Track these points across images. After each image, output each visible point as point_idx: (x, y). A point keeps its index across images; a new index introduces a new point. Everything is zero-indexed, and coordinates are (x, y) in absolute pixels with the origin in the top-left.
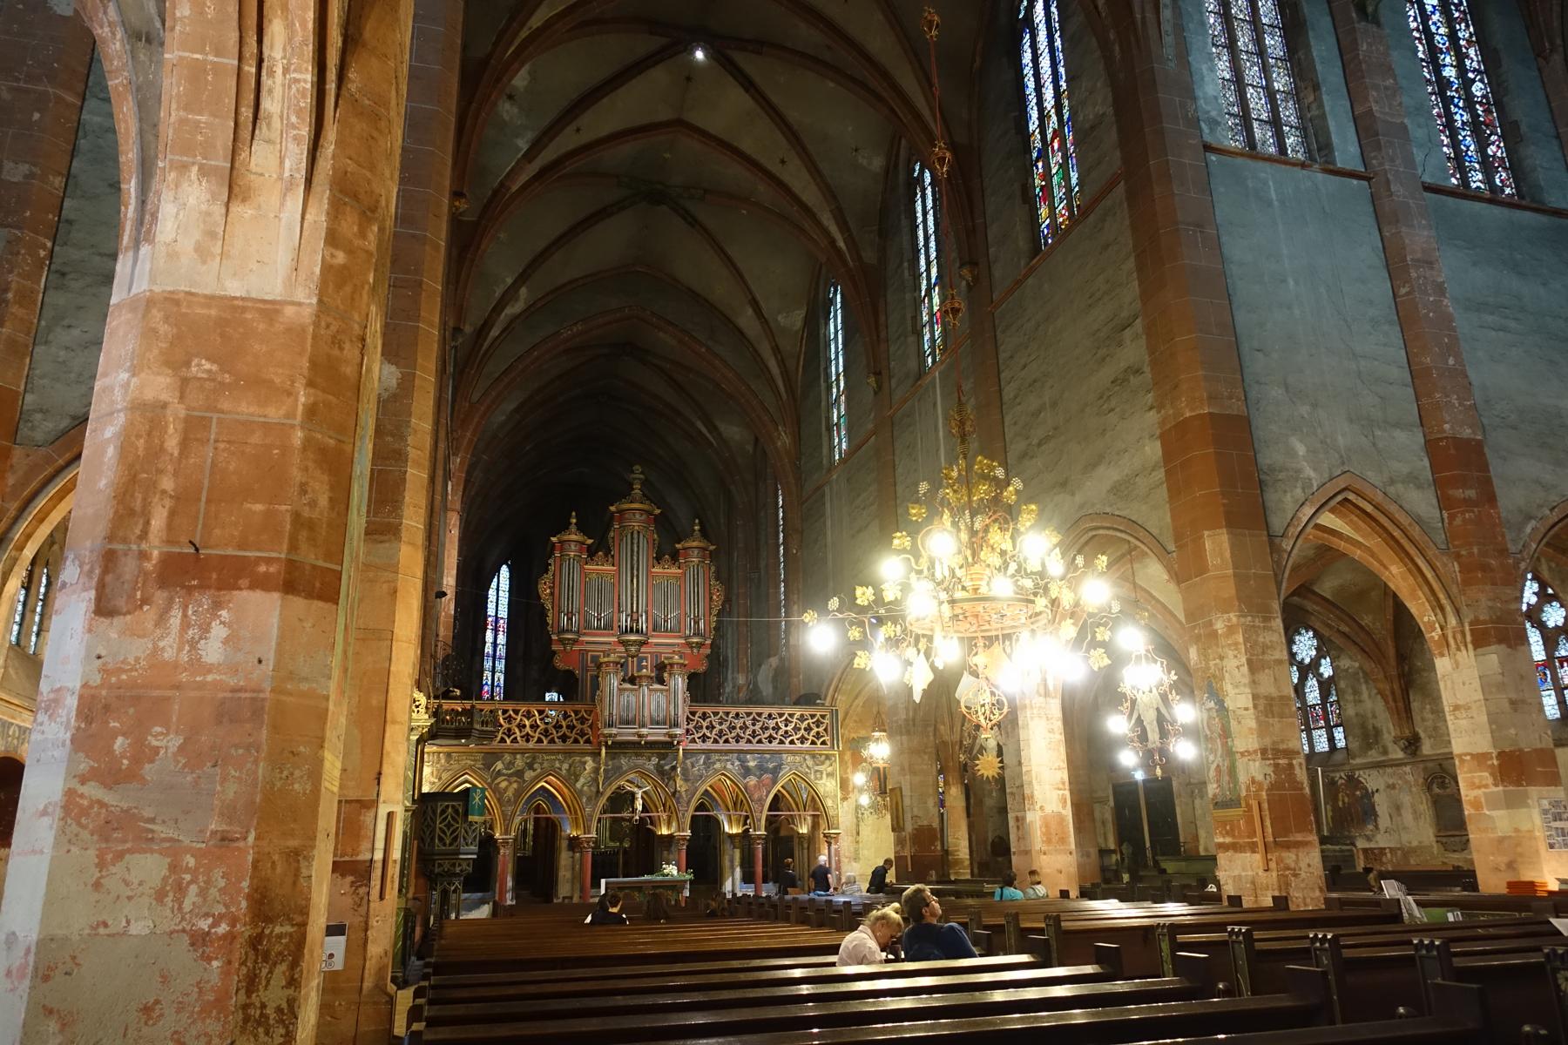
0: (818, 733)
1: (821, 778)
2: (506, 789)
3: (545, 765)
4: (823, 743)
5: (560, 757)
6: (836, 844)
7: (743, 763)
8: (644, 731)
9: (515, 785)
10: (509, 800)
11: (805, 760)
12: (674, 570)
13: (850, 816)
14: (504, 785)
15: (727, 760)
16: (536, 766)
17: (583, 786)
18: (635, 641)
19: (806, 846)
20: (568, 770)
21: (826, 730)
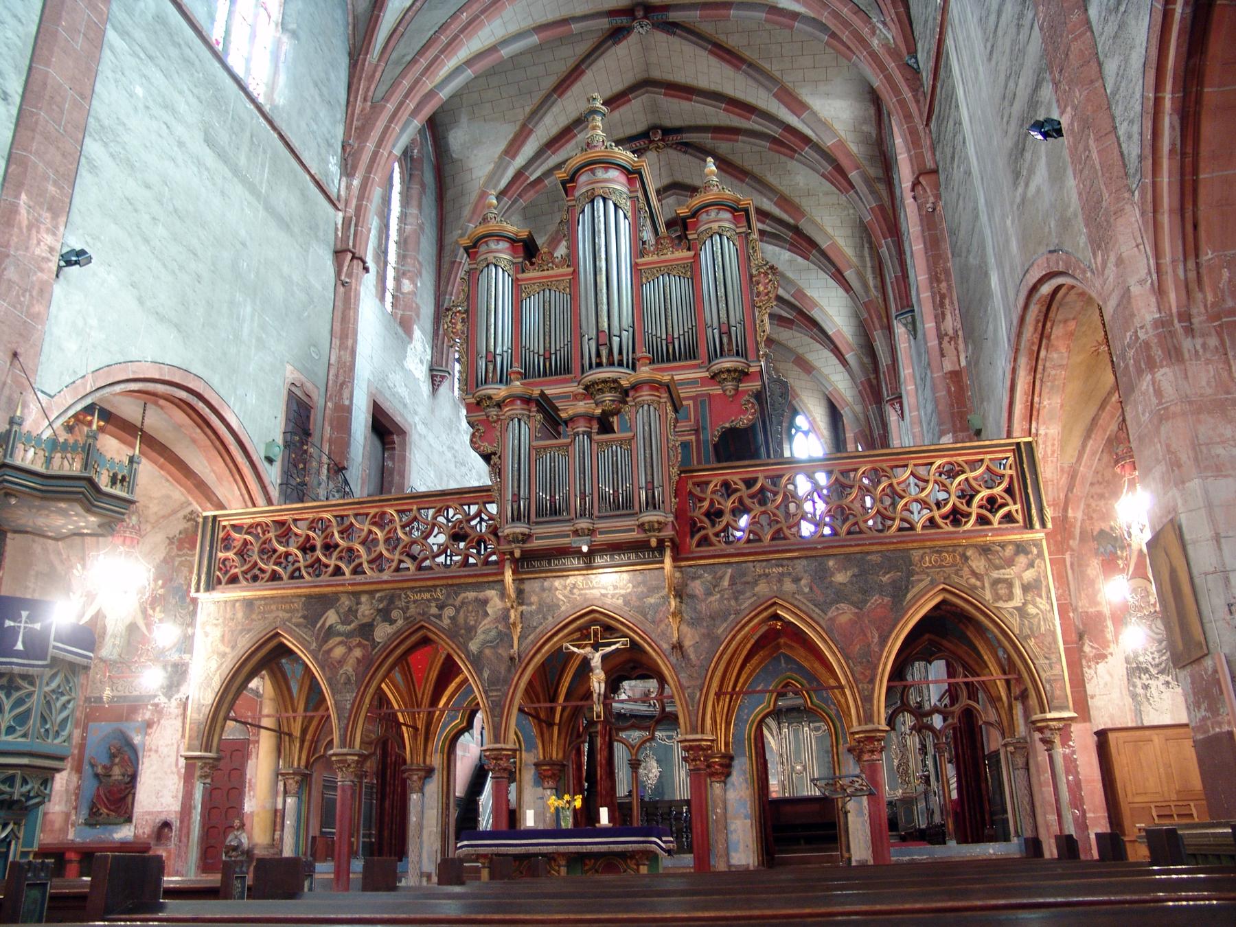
0: (991, 500)
1: (1010, 597)
2: (341, 662)
3: (412, 610)
4: (1009, 518)
5: (439, 594)
6: (1064, 743)
7: (821, 575)
8: (583, 524)
9: (358, 653)
10: (348, 681)
11: (967, 559)
12: (683, 254)
13: (1115, 695)
14: (339, 652)
15: (782, 575)
16: (395, 614)
17: (484, 644)
18: (605, 381)
19: (1020, 761)
20: (452, 619)
21: (1009, 491)
